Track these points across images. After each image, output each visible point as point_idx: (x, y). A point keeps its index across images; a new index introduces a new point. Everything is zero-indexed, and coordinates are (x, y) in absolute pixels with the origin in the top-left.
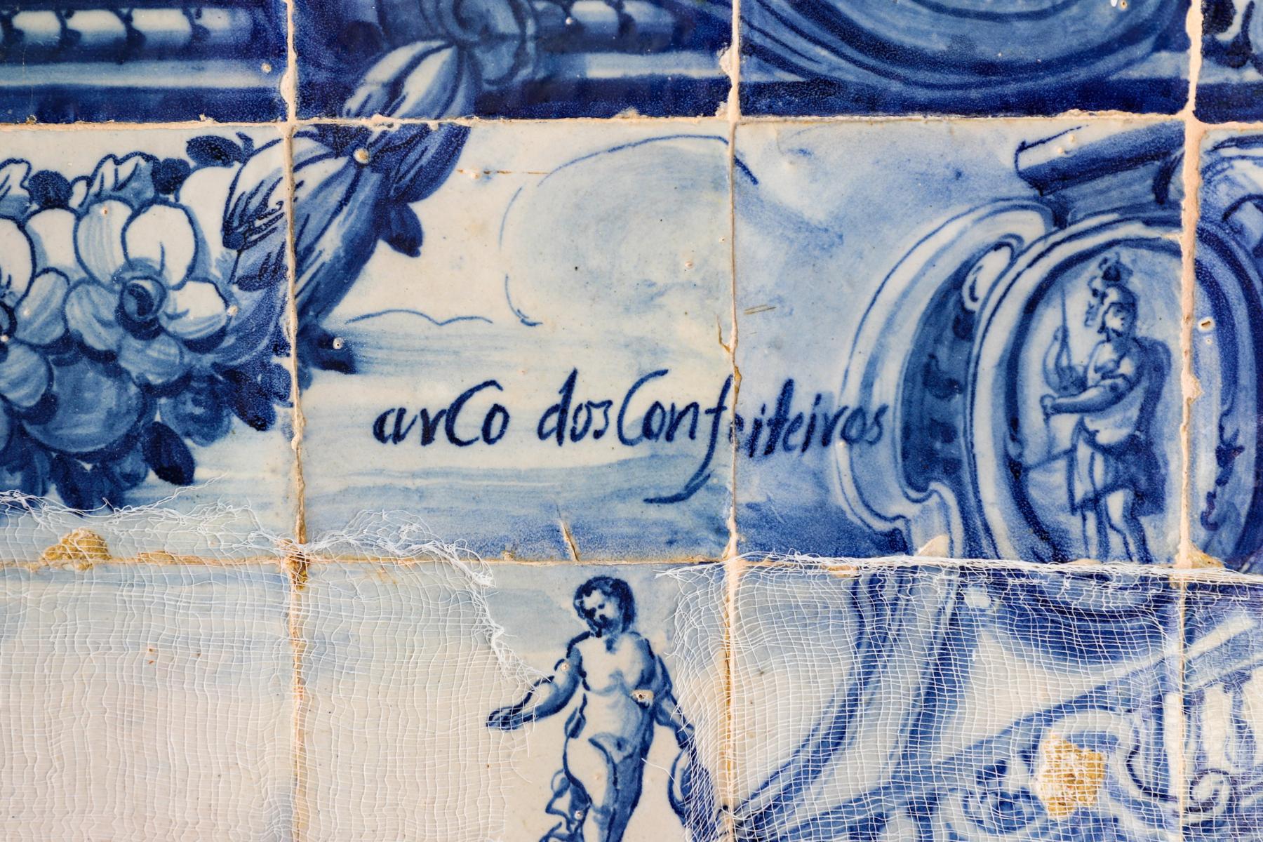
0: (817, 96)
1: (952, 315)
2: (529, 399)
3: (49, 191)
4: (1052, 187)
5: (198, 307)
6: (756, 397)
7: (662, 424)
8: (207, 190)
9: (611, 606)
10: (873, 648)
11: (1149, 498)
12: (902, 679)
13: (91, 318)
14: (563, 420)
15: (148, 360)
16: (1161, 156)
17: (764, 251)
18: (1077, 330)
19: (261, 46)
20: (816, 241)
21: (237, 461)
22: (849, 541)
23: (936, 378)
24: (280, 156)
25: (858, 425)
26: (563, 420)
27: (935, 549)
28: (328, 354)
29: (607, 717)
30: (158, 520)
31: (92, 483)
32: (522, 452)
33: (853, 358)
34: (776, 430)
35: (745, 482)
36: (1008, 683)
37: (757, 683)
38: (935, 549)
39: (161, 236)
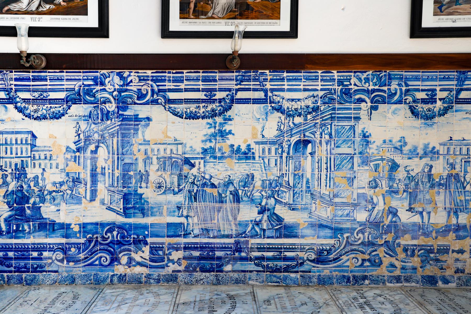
0: (86, 104)
1: (91, 112)
2: (74, 115)
3: (56, 107)
4: (94, 107)
5: (61, 112)
6: (83, 115)
7: (80, 116)
8: (62, 107)
9: (78, 123)
10: (88, 125)
11: (98, 119)
12: (89, 126)
13: (57, 112)
14: (76, 116)
15: (60, 114)
16: (98, 106)
17: (84, 110)
18: (95, 112)
19: (64, 102)
20: (86, 109)
21: (63, 117)
22: (87, 120)
23: (90, 114)
24: (65, 106)
25: (87, 116)
26: (76, 116)
27: (90, 121)
28: (66, 113)
29: (78, 127)
30: (60, 120)
31: (57, 119)
32: (74, 117)
33: (87, 113)
34: (84, 116)
35: (83, 118)
36: (93, 126)
37: (83, 126)
38: (90, 121)
39: (60, 109)
